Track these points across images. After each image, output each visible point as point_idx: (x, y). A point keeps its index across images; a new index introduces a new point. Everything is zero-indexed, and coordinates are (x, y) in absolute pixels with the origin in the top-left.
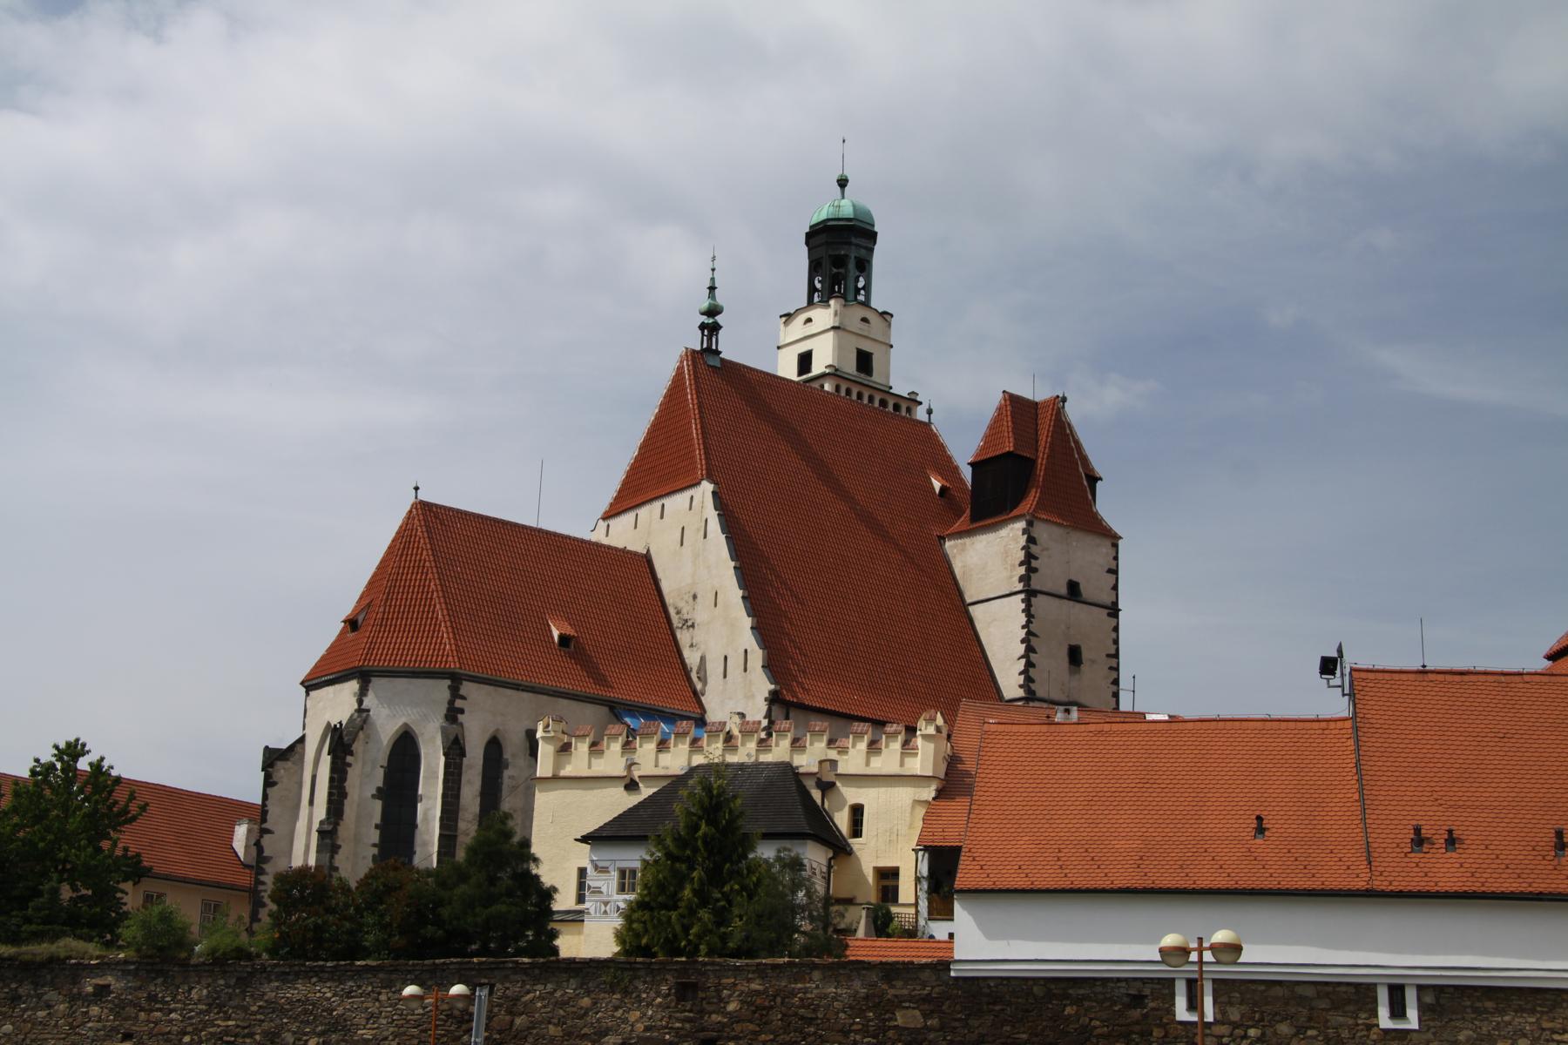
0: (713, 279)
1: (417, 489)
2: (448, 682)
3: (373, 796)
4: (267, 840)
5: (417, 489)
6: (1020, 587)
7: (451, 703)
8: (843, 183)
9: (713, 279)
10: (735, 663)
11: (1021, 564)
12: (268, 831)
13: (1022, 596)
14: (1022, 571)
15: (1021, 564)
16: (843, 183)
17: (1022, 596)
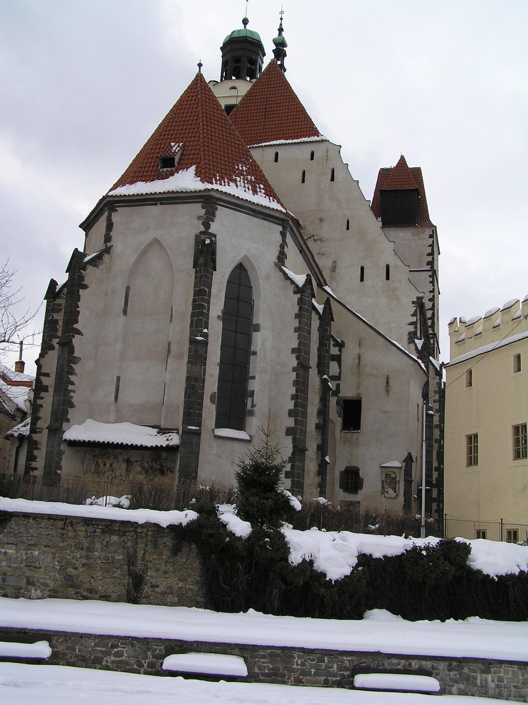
0: (281, 24)
1: (200, 65)
2: (280, 228)
3: (218, 317)
4: (76, 341)
5: (200, 65)
6: (428, 268)
7: (282, 247)
8: (245, 22)
9: (281, 24)
10: (375, 275)
11: (429, 255)
12: (79, 332)
13: (430, 273)
14: (430, 258)
15: (429, 255)
16: (245, 22)
17: (430, 273)
